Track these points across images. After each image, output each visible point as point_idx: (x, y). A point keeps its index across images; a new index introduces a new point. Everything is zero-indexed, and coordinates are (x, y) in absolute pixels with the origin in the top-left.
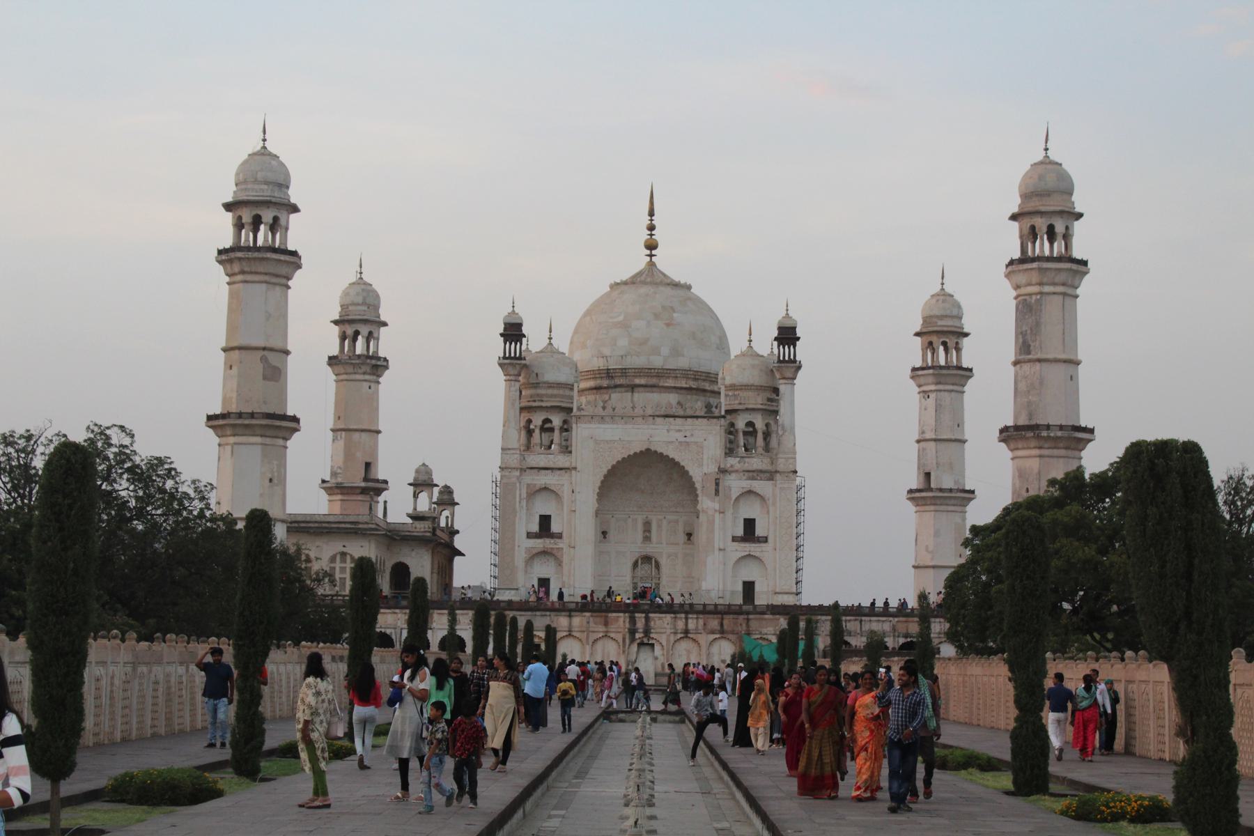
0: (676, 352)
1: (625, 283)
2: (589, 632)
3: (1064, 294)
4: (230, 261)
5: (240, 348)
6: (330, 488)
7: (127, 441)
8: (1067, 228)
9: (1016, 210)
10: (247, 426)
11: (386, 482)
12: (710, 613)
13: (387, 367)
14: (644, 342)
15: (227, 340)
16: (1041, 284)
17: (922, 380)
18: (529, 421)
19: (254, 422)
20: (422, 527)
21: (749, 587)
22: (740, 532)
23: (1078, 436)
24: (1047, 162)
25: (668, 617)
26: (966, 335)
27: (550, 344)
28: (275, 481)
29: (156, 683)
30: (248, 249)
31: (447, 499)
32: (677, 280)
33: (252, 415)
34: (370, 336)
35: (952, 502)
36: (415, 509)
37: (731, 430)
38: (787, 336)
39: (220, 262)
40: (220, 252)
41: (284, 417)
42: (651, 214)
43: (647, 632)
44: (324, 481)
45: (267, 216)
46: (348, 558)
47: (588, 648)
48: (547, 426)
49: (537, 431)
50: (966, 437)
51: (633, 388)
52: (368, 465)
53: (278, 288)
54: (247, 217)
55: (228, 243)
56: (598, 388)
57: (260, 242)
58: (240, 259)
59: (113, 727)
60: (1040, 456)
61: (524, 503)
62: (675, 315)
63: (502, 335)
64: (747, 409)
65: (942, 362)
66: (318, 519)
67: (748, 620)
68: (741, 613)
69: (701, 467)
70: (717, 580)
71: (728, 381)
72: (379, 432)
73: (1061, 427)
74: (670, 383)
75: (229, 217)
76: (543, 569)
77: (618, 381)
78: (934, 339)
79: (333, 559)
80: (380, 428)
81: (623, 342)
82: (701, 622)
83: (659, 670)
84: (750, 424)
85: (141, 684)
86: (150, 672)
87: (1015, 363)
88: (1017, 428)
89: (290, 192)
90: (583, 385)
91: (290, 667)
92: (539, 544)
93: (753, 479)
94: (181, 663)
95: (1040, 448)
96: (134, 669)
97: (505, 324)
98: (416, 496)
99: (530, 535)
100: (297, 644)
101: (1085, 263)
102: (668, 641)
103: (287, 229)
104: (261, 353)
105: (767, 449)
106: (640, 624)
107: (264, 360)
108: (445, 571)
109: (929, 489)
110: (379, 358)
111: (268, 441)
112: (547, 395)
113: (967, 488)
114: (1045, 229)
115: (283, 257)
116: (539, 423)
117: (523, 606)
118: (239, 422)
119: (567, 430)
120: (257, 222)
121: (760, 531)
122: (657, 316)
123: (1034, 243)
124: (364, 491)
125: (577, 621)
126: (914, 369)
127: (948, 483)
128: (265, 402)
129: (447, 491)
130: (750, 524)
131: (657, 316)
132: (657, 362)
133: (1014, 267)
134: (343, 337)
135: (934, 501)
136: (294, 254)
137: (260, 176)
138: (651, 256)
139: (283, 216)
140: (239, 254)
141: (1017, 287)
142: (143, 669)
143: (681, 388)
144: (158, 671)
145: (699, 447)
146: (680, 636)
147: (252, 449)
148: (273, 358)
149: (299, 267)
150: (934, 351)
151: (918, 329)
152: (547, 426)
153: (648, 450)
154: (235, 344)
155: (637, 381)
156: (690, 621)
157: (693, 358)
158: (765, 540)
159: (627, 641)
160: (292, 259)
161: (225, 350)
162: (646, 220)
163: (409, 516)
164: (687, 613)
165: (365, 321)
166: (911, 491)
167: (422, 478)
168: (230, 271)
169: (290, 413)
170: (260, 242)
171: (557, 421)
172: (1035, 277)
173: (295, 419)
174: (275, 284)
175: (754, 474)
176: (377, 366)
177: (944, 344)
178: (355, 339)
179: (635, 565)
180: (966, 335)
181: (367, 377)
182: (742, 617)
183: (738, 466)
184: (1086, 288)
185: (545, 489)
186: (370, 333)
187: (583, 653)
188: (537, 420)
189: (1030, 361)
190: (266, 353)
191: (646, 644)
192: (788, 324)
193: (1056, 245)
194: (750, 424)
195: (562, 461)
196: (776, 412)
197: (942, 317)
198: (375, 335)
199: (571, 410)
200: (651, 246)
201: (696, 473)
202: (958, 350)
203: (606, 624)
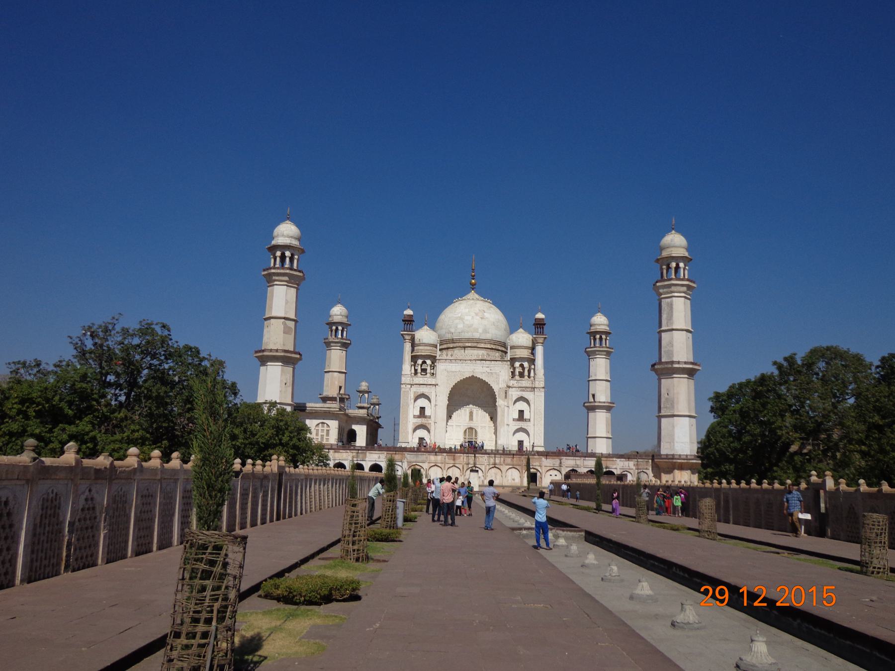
0: (485, 331)
2: (445, 463)
7: (166, 333)
14: (470, 326)
20: (363, 412)
21: (521, 443)
22: (516, 416)
33: (277, 351)
43: (475, 464)
51: (465, 347)
56: (448, 348)
61: (413, 401)
69: (497, 387)
71: (512, 344)
73: (686, 363)
74: (483, 345)
76: (422, 433)
77: (457, 345)
81: (460, 326)
84: (522, 366)
92: (420, 421)
99: (415, 417)
105: (529, 377)
106: (471, 461)
107: (285, 324)
117: (411, 450)
122: (477, 314)
125: (439, 458)
130: (521, 412)
131: (477, 314)
132: (476, 336)
133: (658, 284)
140: (273, 271)
145: (497, 375)
149: (303, 278)
150: (595, 339)
155: (467, 344)
165: (341, 323)
171: (429, 362)
175: (524, 389)
179: (465, 431)
183: (516, 385)
192: (540, 316)
195: (431, 381)
196: (534, 360)
201: (496, 388)
203: (454, 460)
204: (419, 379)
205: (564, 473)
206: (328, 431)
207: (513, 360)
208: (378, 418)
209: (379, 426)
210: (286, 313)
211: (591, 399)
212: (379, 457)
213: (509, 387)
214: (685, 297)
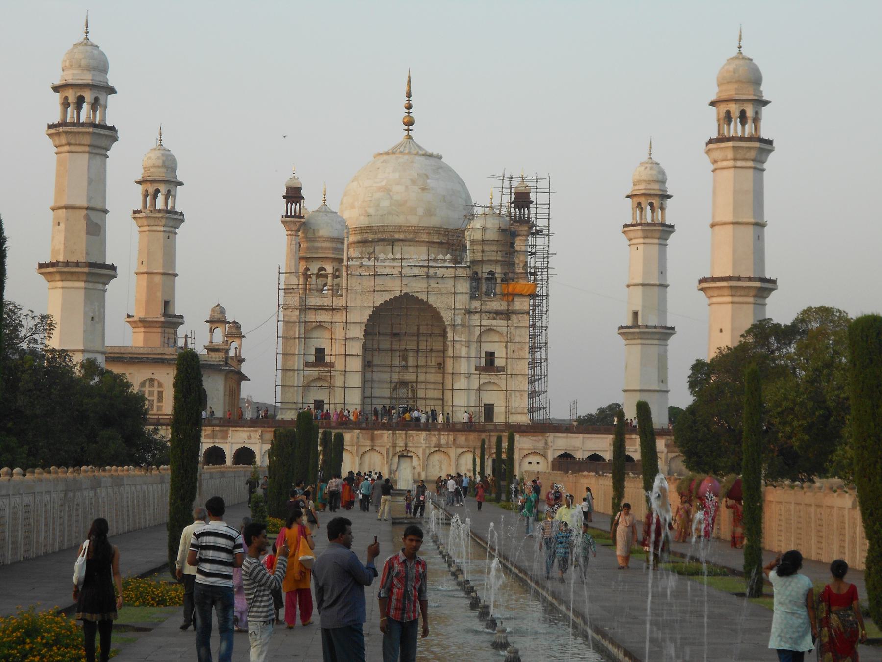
0: (429, 213)
1: (387, 153)
3: (755, 168)
4: (58, 134)
5: (66, 208)
6: (135, 322)
8: (756, 113)
9: (714, 97)
10: (72, 273)
11: (182, 317)
12: (459, 430)
13: (183, 221)
15: (56, 201)
16: (735, 159)
17: (631, 235)
18: (307, 269)
20: (217, 357)
23: (765, 287)
24: (740, 57)
25: (424, 434)
26: (669, 197)
27: (325, 205)
28: (96, 319)
29: (78, 505)
30: (73, 124)
31: (235, 332)
32: (430, 150)
33: (77, 264)
34: (168, 194)
35: (657, 337)
36: (211, 342)
37: (475, 278)
38: (522, 200)
39: (49, 135)
40: (50, 127)
41: (104, 266)
42: (409, 95)
43: (406, 445)
44: (129, 316)
45: (89, 96)
46: (156, 383)
47: (357, 459)
48: (323, 272)
49: (314, 277)
50: (668, 283)
51: (393, 242)
52: (166, 303)
53: (98, 157)
54: (72, 99)
55: (56, 119)
56: (364, 242)
57: (83, 119)
58: (66, 133)
59: (54, 540)
60: (732, 303)
62: (429, 181)
63: (284, 197)
64: (488, 261)
65: (649, 221)
66: (130, 350)
67: (490, 436)
68: (484, 431)
70: (462, 404)
72: (176, 275)
73: (750, 279)
74: (425, 238)
75: (57, 97)
77: (380, 236)
78: (643, 200)
79: (143, 384)
80: (177, 272)
81: (385, 204)
82: (451, 438)
83: (416, 477)
85: (69, 507)
86: (74, 496)
87: (713, 225)
88: (714, 279)
89: (109, 76)
90: (352, 239)
91: (155, 486)
92: (313, 372)
93: (494, 319)
94: (92, 489)
95: (732, 296)
96: (66, 495)
97: (288, 188)
98: (211, 331)
100: (158, 467)
101: (770, 142)
102: (424, 453)
103: (105, 107)
104: (84, 212)
107: (87, 218)
108: (233, 393)
109: (639, 327)
110: (176, 213)
111: (90, 286)
112: (322, 248)
113: (669, 325)
114: (738, 114)
115: (103, 132)
116: (316, 271)
118: (66, 269)
119: (337, 277)
120: (80, 101)
121: (498, 363)
123: (729, 124)
124: (163, 325)
126: (625, 226)
127: (653, 321)
128: (87, 254)
129: (236, 325)
130: (491, 355)
131: (414, 182)
132: (413, 220)
133: (711, 146)
134: (146, 196)
135: (643, 336)
136: (112, 129)
137: (83, 62)
138: (409, 130)
139: (102, 97)
141: (715, 162)
142: (71, 494)
143: (434, 243)
144: (78, 494)
146: (433, 450)
148: (94, 216)
151: (629, 193)
152: (323, 272)
153: (406, 294)
154: (62, 204)
155: (397, 236)
156: (442, 437)
157: (444, 217)
158: (503, 369)
159: (391, 455)
160: (108, 134)
162: (404, 101)
163: (206, 347)
164: (439, 430)
166: (622, 327)
167: (217, 316)
168: (57, 143)
169: (108, 262)
170: (83, 119)
171: (329, 269)
172: (730, 154)
173: (113, 268)
174: (96, 154)
176: (174, 218)
177: (651, 204)
178: (155, 196)
180: (669, 197)
181: (166, 229)
182: (484, 436)
184: (772, 162)
185: (320, 325)
186: (169, 191)
187: (353, 463)
188: (314, 268)
189: (725, 224)
190: (89, 212)
191: (404, 455)
193: (747, 127)
194: (491, 273)
197: (649, 182)
198: (173, 193)
199: (343, 260)
200: (409, 123)
202: (662, 208)
203: (373, 439)
204: (314, 301)
205: (550, 459)
206: (160, 394)
207: (474, 262)
208: (242, 361)
209: (245, 378)
210: (89, 199)
211: (628, 321)
212: (250, 437)
213: (469, 312)
214: (755, 168)
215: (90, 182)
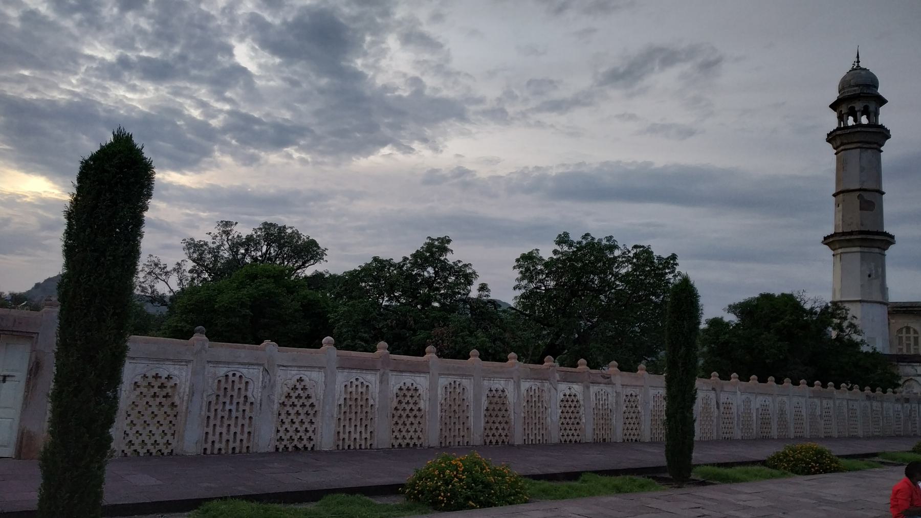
10: (848, 240)
19: (853, 237)
28: (873, 276)
33: (851, 233)
53: (869, 151)
58: (839, 135)
104: (858, 193)
111: (866, 250)
118: (843, 238)
128: (862, 225)
137: (852, 82)
140: (839, 132)
147: (854, 255)
148: (866, 196)
149: (888, 137)
160: (884, 134)
161: (834, 195)
215: (862, 169)
